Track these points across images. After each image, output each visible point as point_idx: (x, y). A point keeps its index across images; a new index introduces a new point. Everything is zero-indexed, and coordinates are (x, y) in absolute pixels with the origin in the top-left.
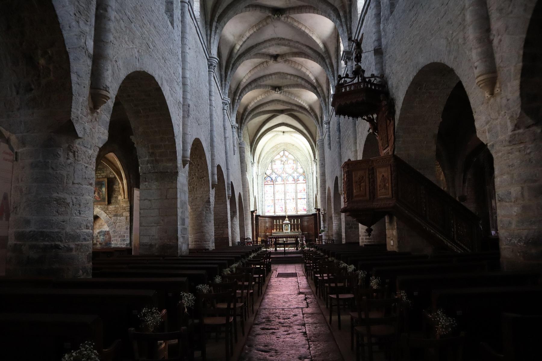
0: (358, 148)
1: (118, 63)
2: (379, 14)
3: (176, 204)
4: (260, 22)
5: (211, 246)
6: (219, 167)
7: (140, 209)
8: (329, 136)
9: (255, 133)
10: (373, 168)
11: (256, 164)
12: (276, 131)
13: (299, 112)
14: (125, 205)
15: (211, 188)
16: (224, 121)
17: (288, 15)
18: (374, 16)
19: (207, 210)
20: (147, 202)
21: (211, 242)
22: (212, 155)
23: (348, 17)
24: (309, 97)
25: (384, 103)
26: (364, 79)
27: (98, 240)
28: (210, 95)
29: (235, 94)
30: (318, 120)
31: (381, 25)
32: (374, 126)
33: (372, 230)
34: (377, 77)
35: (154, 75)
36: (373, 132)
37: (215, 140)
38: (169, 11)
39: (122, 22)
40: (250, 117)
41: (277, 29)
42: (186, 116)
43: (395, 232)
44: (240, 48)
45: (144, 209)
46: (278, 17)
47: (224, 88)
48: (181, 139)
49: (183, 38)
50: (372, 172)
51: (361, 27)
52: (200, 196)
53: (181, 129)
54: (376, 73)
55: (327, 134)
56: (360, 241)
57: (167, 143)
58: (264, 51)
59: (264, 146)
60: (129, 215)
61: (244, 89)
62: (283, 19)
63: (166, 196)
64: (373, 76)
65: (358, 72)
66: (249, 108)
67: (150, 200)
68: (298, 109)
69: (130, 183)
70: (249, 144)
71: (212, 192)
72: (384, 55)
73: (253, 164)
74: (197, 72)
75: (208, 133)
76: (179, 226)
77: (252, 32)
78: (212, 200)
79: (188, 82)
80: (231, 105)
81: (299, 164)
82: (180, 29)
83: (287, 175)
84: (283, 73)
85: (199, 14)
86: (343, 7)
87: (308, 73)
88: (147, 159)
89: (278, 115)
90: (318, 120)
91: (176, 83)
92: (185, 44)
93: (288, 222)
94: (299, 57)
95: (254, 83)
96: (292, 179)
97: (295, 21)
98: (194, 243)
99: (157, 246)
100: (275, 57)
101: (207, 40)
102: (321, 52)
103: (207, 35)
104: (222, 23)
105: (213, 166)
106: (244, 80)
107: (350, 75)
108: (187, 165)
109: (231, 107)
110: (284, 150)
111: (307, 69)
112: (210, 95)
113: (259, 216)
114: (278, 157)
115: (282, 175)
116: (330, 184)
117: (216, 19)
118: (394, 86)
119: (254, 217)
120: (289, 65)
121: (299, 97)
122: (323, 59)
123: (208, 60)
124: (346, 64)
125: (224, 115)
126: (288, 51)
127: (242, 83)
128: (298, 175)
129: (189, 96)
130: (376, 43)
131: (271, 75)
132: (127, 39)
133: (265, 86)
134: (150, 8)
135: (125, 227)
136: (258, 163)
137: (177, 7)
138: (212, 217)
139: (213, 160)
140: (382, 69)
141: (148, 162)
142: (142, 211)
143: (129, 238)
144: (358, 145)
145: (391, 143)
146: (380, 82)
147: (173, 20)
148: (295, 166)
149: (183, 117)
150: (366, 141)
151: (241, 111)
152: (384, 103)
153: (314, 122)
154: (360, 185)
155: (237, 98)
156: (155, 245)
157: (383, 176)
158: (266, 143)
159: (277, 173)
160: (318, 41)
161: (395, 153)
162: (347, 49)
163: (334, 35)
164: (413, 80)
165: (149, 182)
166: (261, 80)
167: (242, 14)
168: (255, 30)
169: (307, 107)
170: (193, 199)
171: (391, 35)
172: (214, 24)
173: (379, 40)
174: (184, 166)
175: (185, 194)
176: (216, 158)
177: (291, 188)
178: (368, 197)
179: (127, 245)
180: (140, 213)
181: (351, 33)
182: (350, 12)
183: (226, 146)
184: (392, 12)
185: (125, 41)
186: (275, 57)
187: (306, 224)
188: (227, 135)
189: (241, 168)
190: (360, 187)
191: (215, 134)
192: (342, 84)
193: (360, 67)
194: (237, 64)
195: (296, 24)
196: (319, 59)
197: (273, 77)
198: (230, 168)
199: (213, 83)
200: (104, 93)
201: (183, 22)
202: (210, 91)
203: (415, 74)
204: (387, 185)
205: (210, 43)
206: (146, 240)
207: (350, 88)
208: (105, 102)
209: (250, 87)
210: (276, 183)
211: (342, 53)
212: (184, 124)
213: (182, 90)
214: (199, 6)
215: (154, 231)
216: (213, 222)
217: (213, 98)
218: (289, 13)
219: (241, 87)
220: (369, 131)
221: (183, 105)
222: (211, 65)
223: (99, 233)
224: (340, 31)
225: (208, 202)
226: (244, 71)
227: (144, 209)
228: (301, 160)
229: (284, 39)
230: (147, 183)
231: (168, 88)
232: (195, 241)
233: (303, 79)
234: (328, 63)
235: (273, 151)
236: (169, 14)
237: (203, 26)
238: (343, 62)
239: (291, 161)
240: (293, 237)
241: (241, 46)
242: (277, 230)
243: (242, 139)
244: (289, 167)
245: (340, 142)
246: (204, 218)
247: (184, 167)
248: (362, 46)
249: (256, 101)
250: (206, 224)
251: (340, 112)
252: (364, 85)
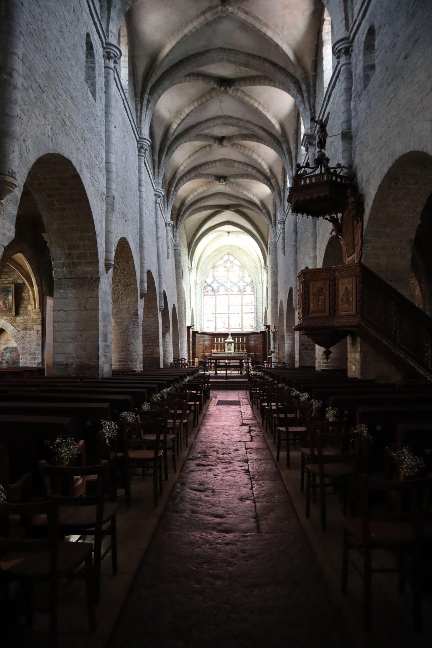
0: (317, 254)
1: (27, 143)
2: (350, 89)
3: (97, 316)
4: (203, 95)
5: (139, 367)
6: (149, 273)
7: (54, 322)
8: (284, 239)
9: (193, 232)
10: (335, 279)
11: (194, 271)
12: (219, 231)
13: (247, 208)
14: (36, 317)
15: (139, 298)
16: (156, 217)
17: (237, 86)
18: (343, 91)
19: (134, 324)
20: (62, 314)
21: (138, 362)
22: (142, 258)
23: (312, 92)
24: (261, 191)
25: (351, 199)
26: (328, 169)
27: (4, 358)
28: (140, 185)
29: (171, 184)
30: (270, 219)
31: (352, 102)
32: (338, 228)
33: (330, 352)
34: (344, 167)
35: (71, 158)
36: (337, 235)
37: (145, 239)
38: (90, 79)
39: (31, 90)
40: (188, 213)
41: (224, 105)
42: (110, 210)
43: (358, 356)
44: (177, 128)
45: (58, 322)
46: (225, 89)
47: (156, 177)
48: (104, 238)
49: (107, 113)
50: (334, 283)
51: (327, 104)
52: (127, 307)
53: (104, 226)
54: (342, 163)
55: (282, 235)
56: (317, 365)
57: (87, 242)
58: (206, 131)
59: (204, 249)
60: (40, 328)
61: (181, 178)
62: (231, 92)
63: (85, 307)
64: (339, 166)
65: (321, 160)
66: (187, 201)
67: (65, 311)
68: (246, 204)
69: (42, 289)
70: (186, 246)
71: (141, 303)
72: (354, 140)
73: (190, 270)
74: (124, 156)
75: (136, 231)
76: (100, 343)
77: (192, 108)
78: (141, 312)
79: (113, 168)
80: (165, 198)
81: (246, 271)
82: (104, 102)
84: (230, 160)
85: (127, 83)
86: (306, 78)
87: (260, 160)
88: (62, 261)
89: (222, 212)
90: (270, 219)
91: (98, 169)
92: (110, 121)
93: (231, 340)
94: (249, 140)
95: (194, 171)
96: (238, 289)
97: (247, 95)
98: (118, 363)
99: (74, 366)
100: (221, 140)
101: (137, 117)
102: (277, 136)
103: (137, 110)
104: (155, 95)
105: (142, 272)
106: (182, 168)
107: (312, 164)
108: (111, 270)
109: (166, 201)
111: (259, 156)
112: (140, 185)
113: (197, 332)
114: (221, 262)
115: (226, 284)
116: (283, 297)
117: (148, 91)
118: (365, 179)
119: (191, 333)
120: (238, 150)
121: (248, 190)
122: (279, 143)
123: (137, 141)
124: (307, 150)
125: (156, 209)
126: (236, 133)
127: (179, 170)
128: (245, 284)
129: (114, 186)
130: (345, 126)
131: (215, 161)
132: (37, 113)
133: (208, 175)
134: (66, 74)
135: (36, 343)
136: (197, 268)
137: (99, 74)
138: (140, 333)
139: (142, 264)
140: (351, 158)
141: (63, 265)
142: (56, 324)
143: (40, 356)
144: (318, 250)
145: (358, 249)
146: (347, 173)
147: (95, 90)
148: (241, 273)
149: (107, 212)
150: (327, 246)
151: (178, 205)
152: (351, 199)
153: (266, 220)
154: (318, 298)
155: (173, 189)
156: (72, 364)
157: (346, 288)
158: (208, 244)
159: (220, 281)
160: (274, 122)
161: (362, 261)
162: (309, 132)
163: (293, 114)
164: (388, 172)
165: (65, 290)
166: (203, 168)
167: (180, 85)
168: (196, 105)
169: (258, 203)
170: (117, 311)
171: (364, 115)
172: (146, 96)
173: (348, 121)
174: (107, 270)
175: (108, 304)
176: (146, 261)
177: (236, 300)
178: (327, 313)
179: (38, 364)
180: (54, 327)
181: (314, 112)
182: (315, 85)
183: (158, 248)
184: (366, 86)
185: (35, 115)
186: (221, 140)
187: (252, 343)
188: (159, 235)
189: (176, 274)
190: (319, 301)
191: (145, 232)
192: (301, 175)
193: (324, 155)
194: (173, 148)
195: (247, 99)
196: (275, 144)
197: (218, 164)
198: (162, 274)
199: (144, 170)
200: (10, 179)
201: (107, 92)
202: (140, 181)
203: (390, 166)
204: (351, 299)
205: (140, 121)
206: (61, 359)
207: (311, 181)
208: (11, 191)
209: (188, 176)
210: (218, 293)
211: (302, 136)
212: (108, 221)
213: (105, 179)
214: (127, 73)
215: (70, 348)
216: (141, 338)
217: (143, 189)
218: (239, 84)
219: (178, 176)
220: (331, 233)
221: (107, 197)
222: (142, 148)
223: (5, 349)
224: (301, 110)
225: (136, 314)
226: (182, 156)
227: (58, 322)
229: (232, 117)
230: (62, 291)
231: (88, 175)
232: (120, 361)
233: (254, 168)
234: (284, 149)
235: (216, 255)
236: (89, 82)
237: (132, 100)
238: (303, 148)
239: (236, 268)
240: (237, 359)
241: (179, 125)
242: (217, 350)
243: (178, 240)
244: (235, 275)
245: (296, 246)
246: (130, 334)
247: (107, 272)
248: (327, 128)
249: (195, 193)
250: (133, 341)
251: (297, 209)
252: (328, 177)
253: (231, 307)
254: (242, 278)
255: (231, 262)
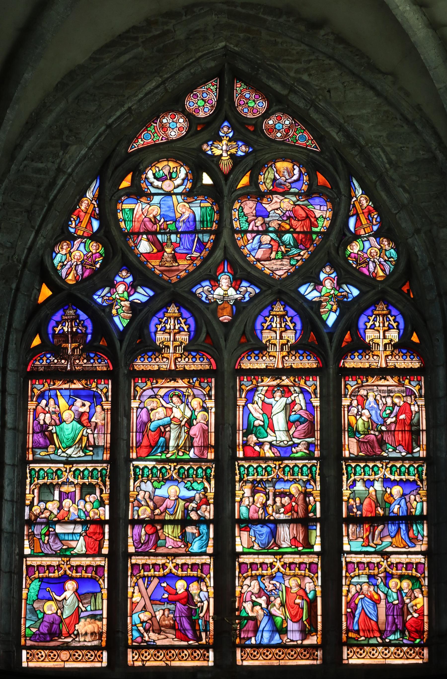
83: (248, 290)
110: (227, 73)
114: (174, 127)
148: (322, 212)
228: (380, 158)
244: (274, 219)
253: (247, 470)
254: (330, 250)
255: (247, 130)
